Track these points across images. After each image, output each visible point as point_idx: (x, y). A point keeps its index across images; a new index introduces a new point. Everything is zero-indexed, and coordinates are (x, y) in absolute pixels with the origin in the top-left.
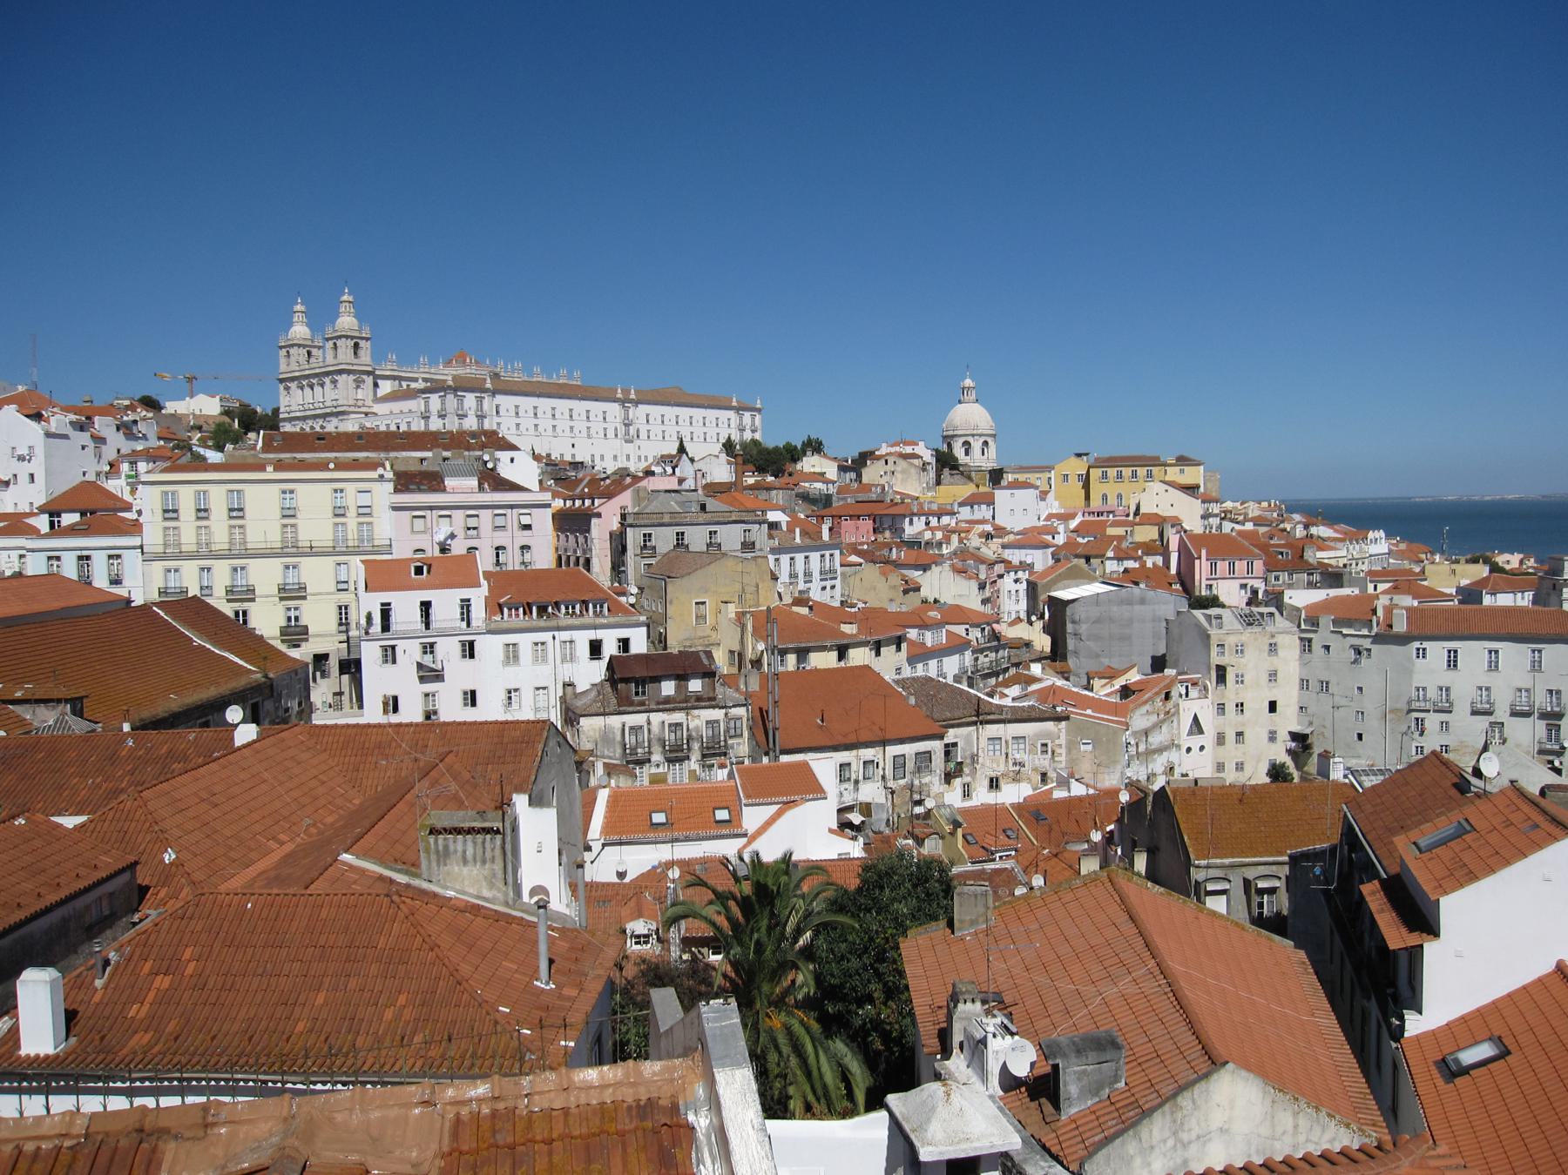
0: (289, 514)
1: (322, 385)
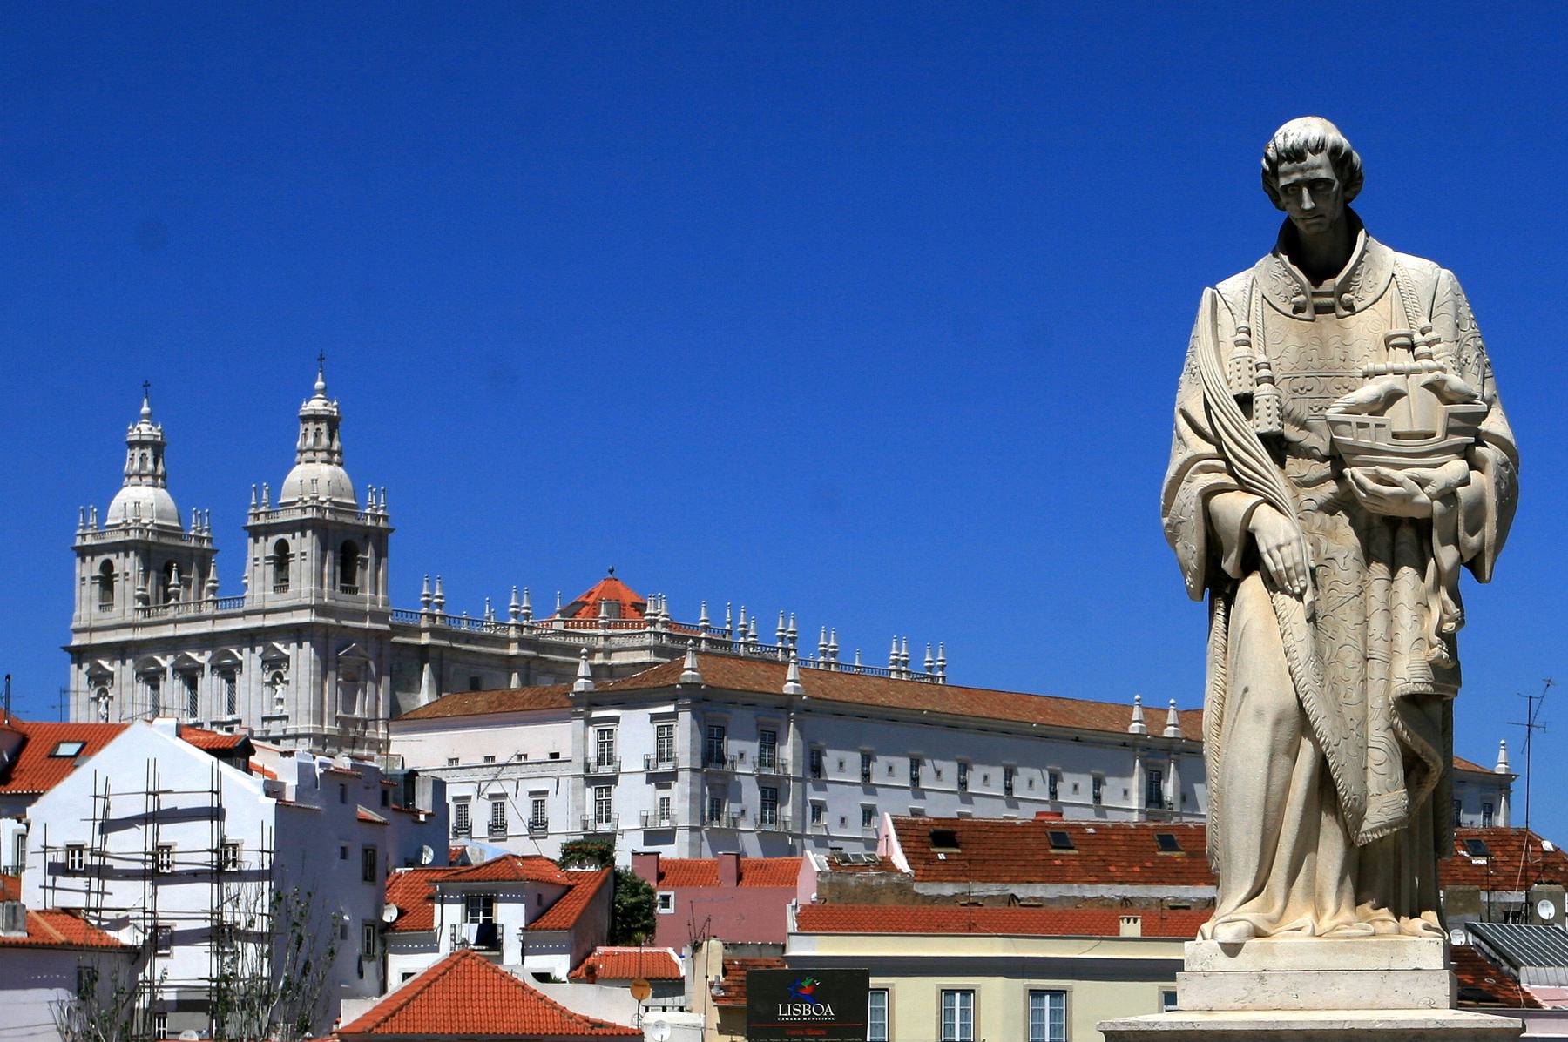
1: (229, 673)
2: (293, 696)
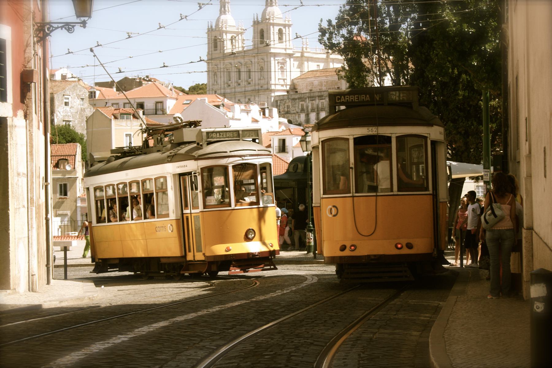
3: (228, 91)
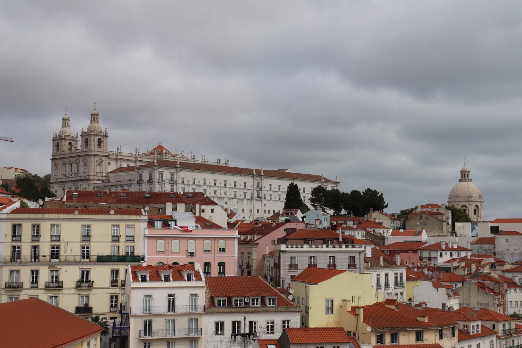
0: (87, 237)
1: (77, 164)
2: (88, 168)
3: (64, 180)
